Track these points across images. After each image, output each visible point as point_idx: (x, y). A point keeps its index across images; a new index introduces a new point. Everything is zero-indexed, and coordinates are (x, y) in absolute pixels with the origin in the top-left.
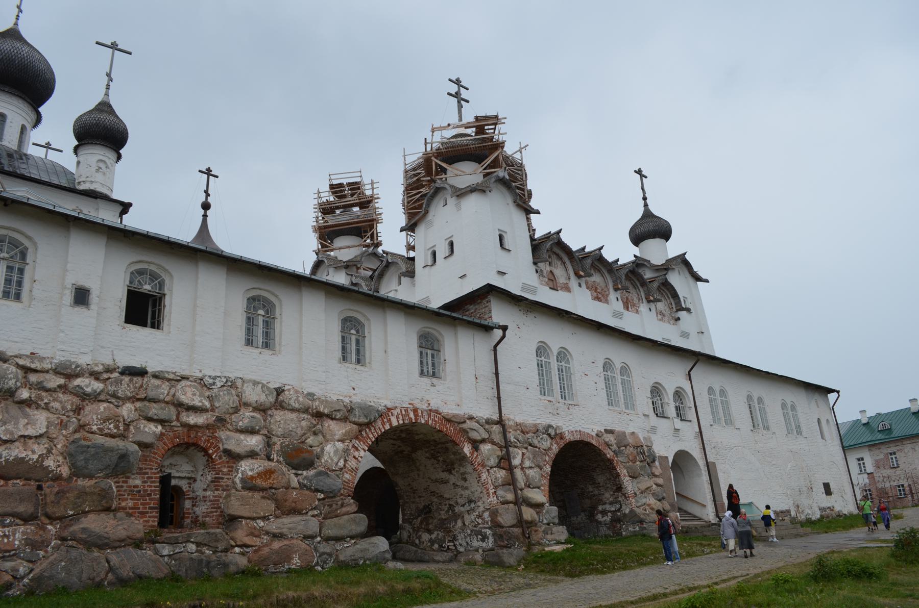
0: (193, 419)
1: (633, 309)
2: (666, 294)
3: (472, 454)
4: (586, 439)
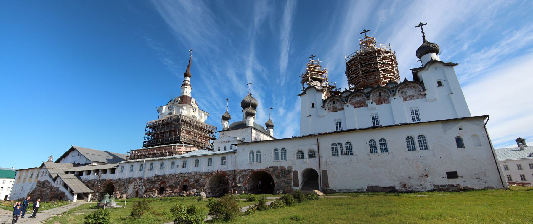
0: (186, 178)
1: (386, 102)
2: (416, 86)
3: (228, 178)
4: (262, 170)
